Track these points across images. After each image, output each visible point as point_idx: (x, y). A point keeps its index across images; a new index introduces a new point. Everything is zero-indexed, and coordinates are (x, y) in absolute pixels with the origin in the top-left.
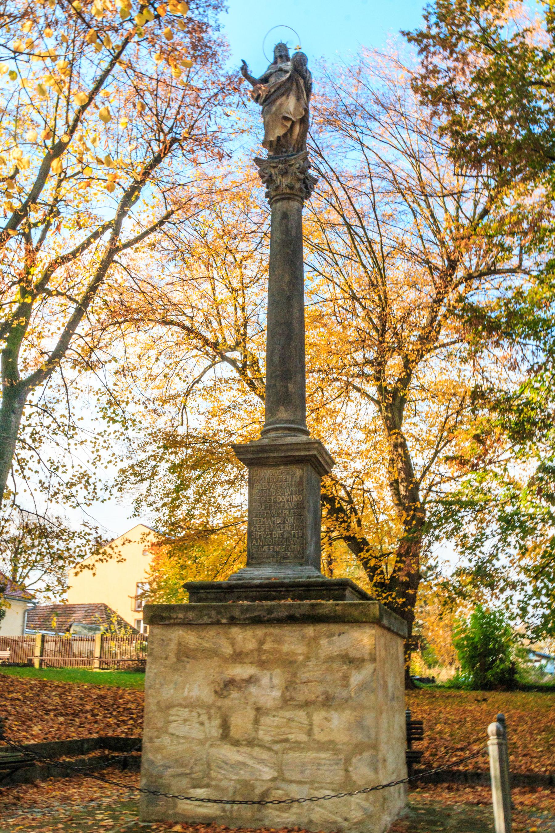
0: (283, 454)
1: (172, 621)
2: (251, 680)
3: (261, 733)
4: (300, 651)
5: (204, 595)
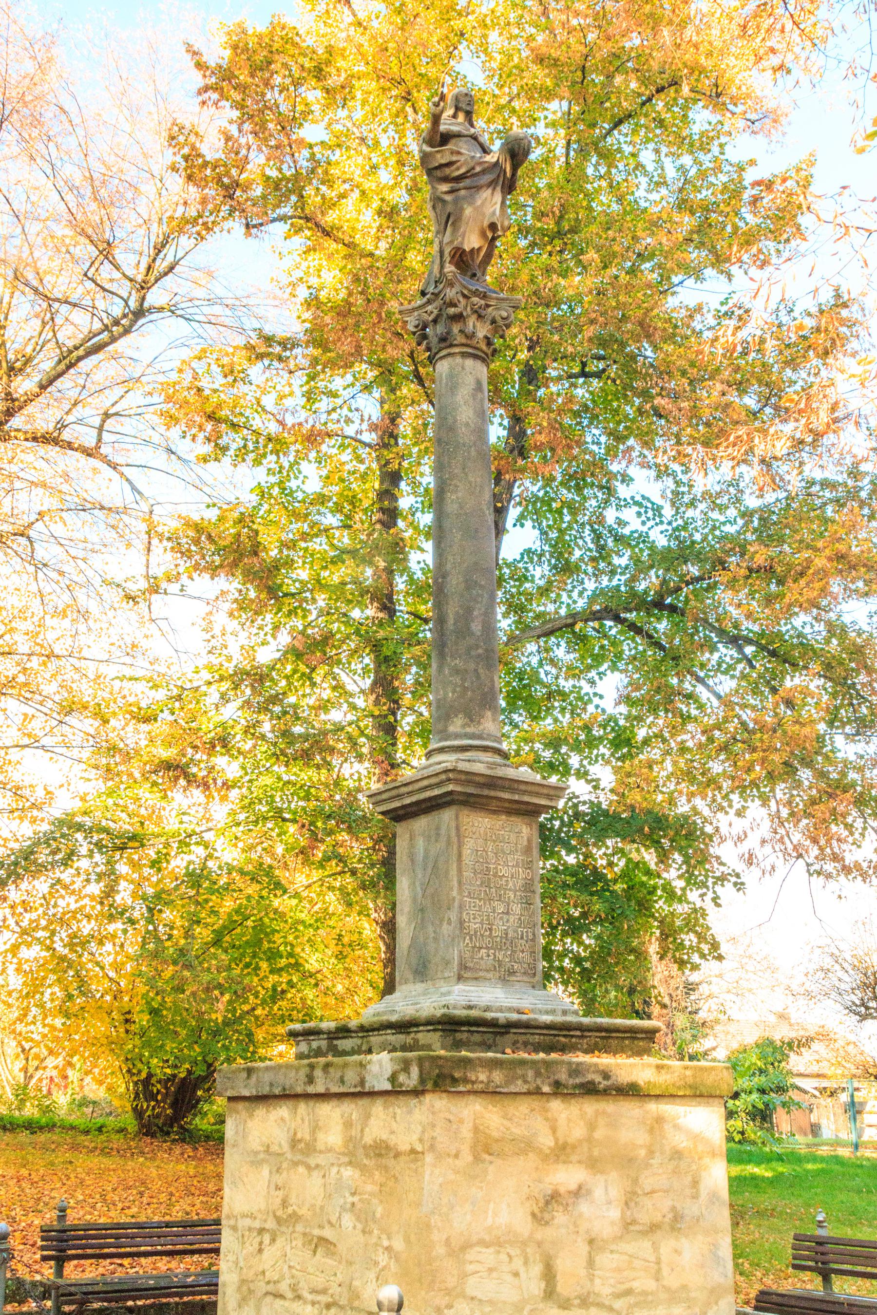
0: (516, 797)
1: (469, 1087)
2: (578, 1192)
3: (597, 1281)
4: (640, 1142)
5: (464, 1036)
